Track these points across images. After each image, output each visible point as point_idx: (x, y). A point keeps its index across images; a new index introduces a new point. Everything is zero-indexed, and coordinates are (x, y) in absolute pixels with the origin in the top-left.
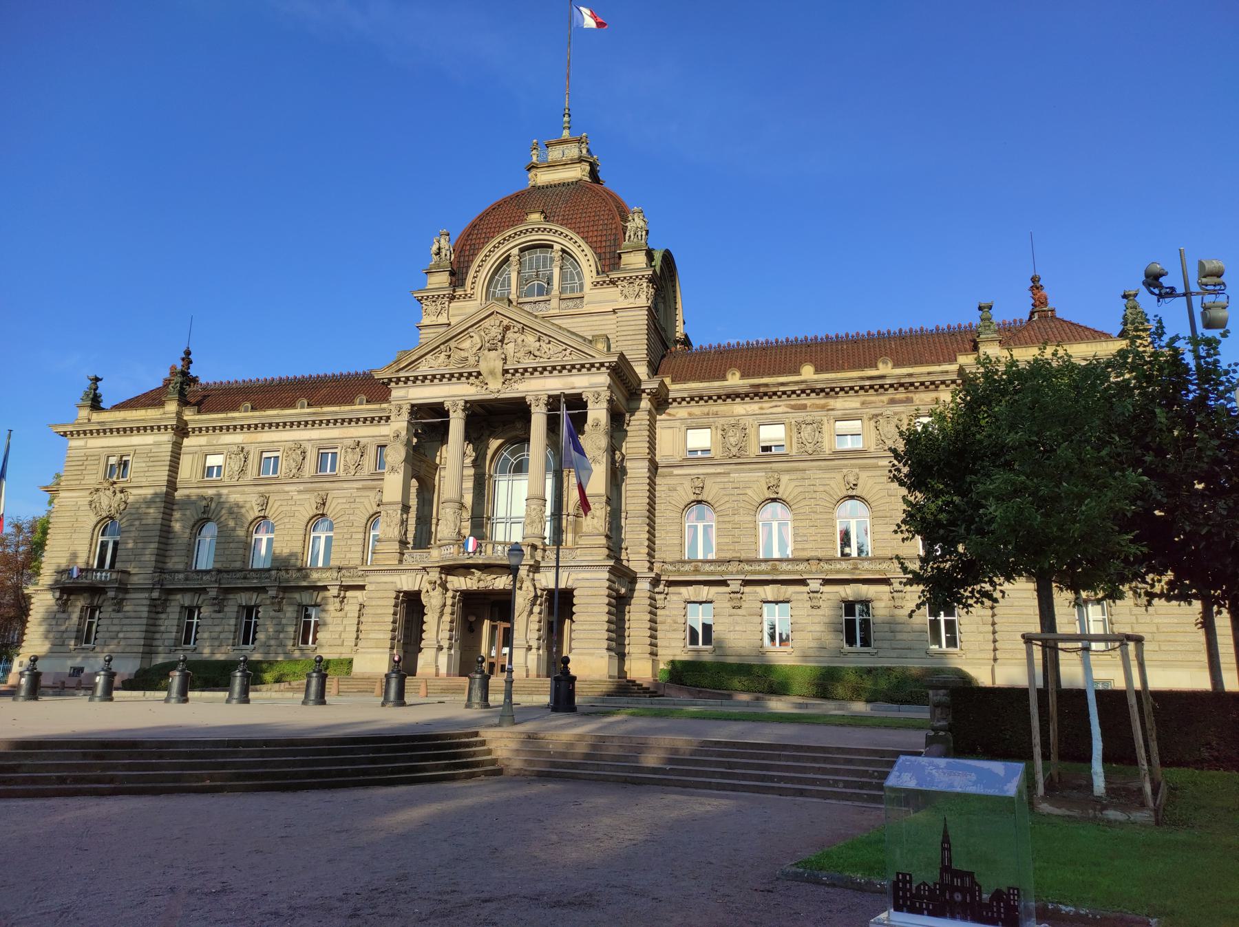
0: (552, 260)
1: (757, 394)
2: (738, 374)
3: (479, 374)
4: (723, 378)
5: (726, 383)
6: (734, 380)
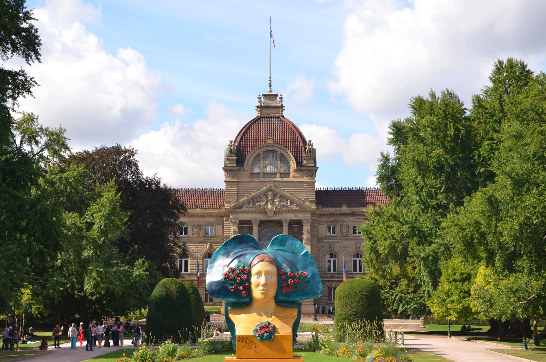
0: (277, 157)
1: (353, 214)
2: (346, 206)
3: (265, 212)
4: (341, 207)
5: (341, 209)
6: (345, 209)
